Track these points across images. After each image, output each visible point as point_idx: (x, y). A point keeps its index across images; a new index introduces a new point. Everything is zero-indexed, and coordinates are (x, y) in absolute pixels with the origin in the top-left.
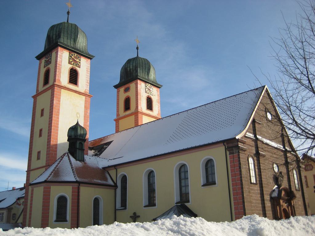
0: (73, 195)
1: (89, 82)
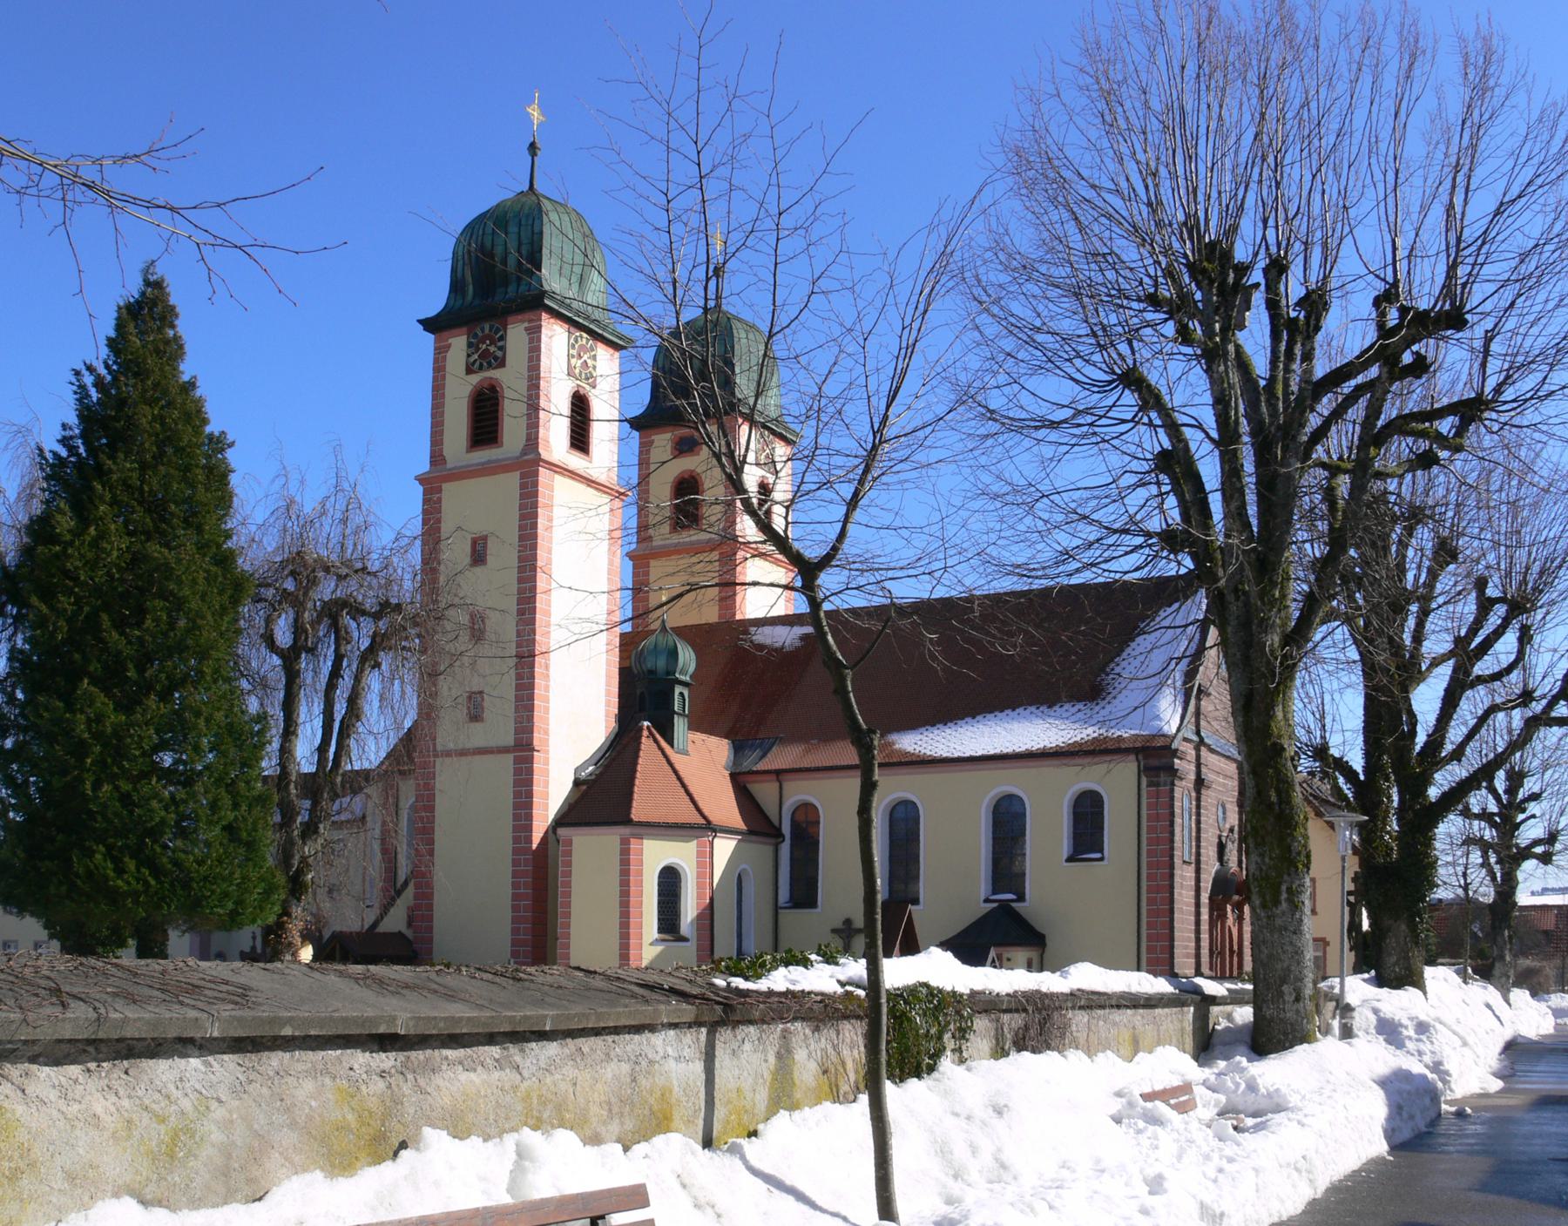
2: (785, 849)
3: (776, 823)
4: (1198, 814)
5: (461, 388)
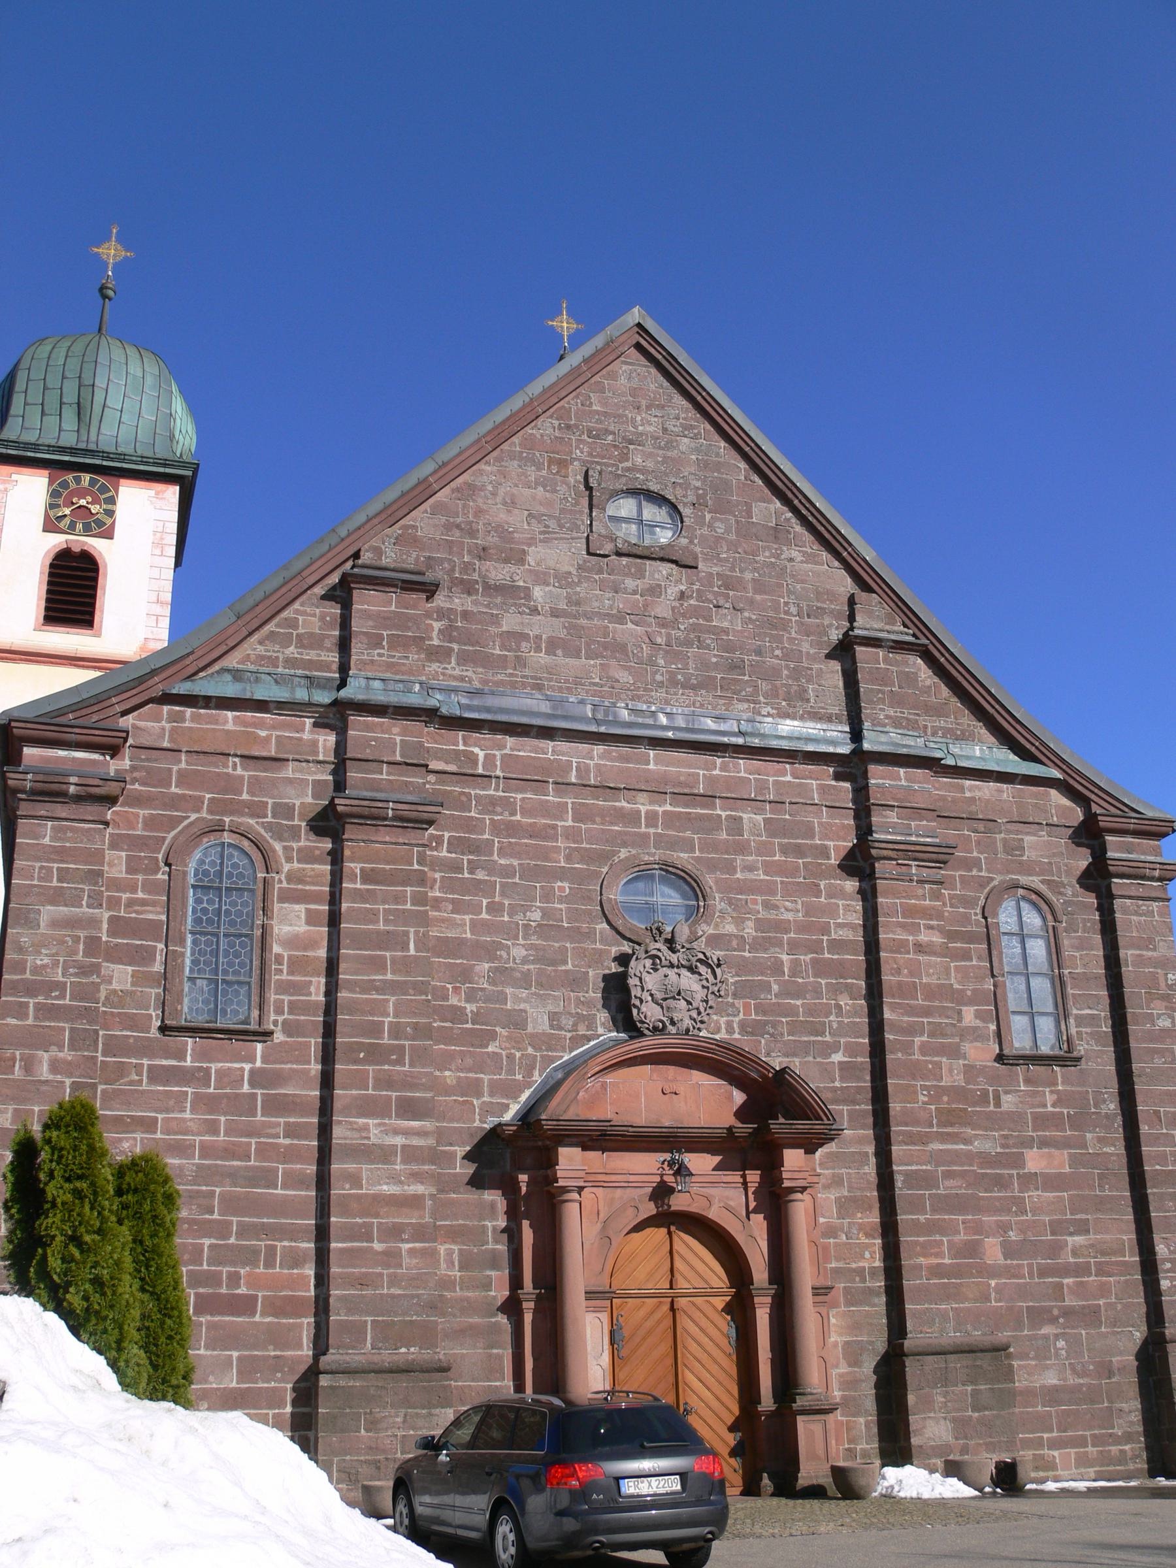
1: (168, 597)
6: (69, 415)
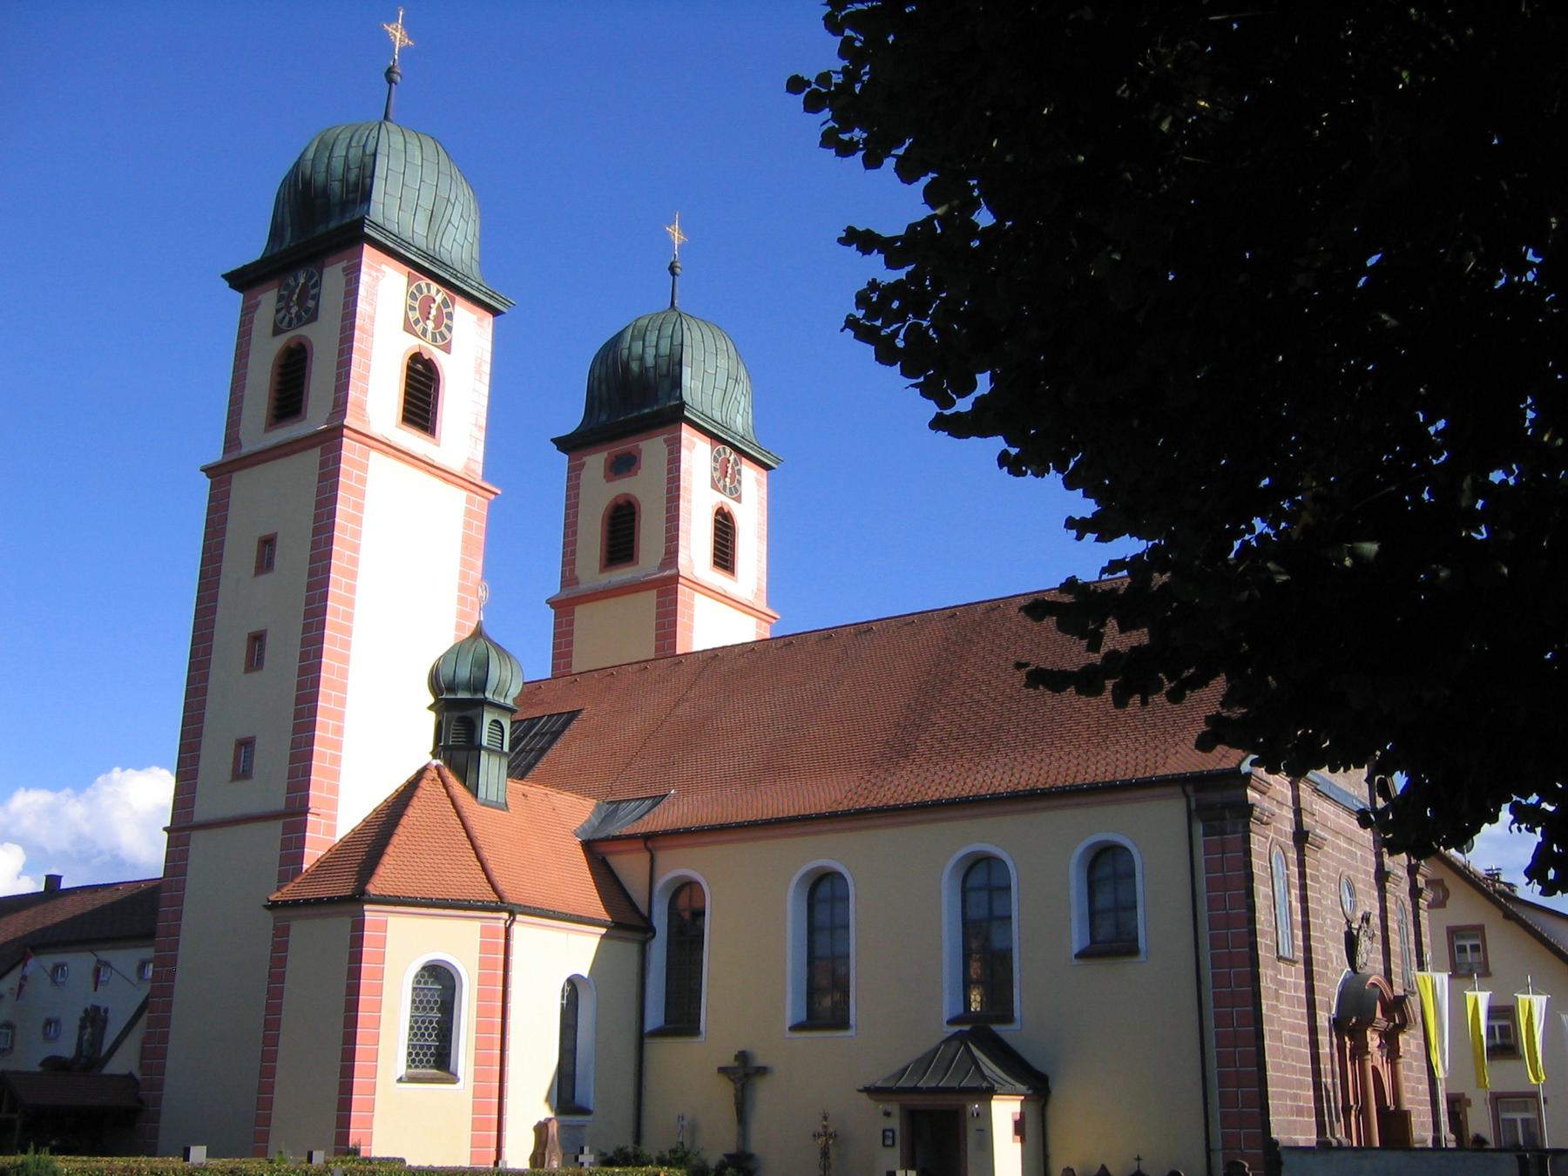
0: (483, 963)
1: (483, 422)
2: (658, 949)
3: (643, 908)
4: (1303, 887)
5: (266, 351)
6: (423, 217)
